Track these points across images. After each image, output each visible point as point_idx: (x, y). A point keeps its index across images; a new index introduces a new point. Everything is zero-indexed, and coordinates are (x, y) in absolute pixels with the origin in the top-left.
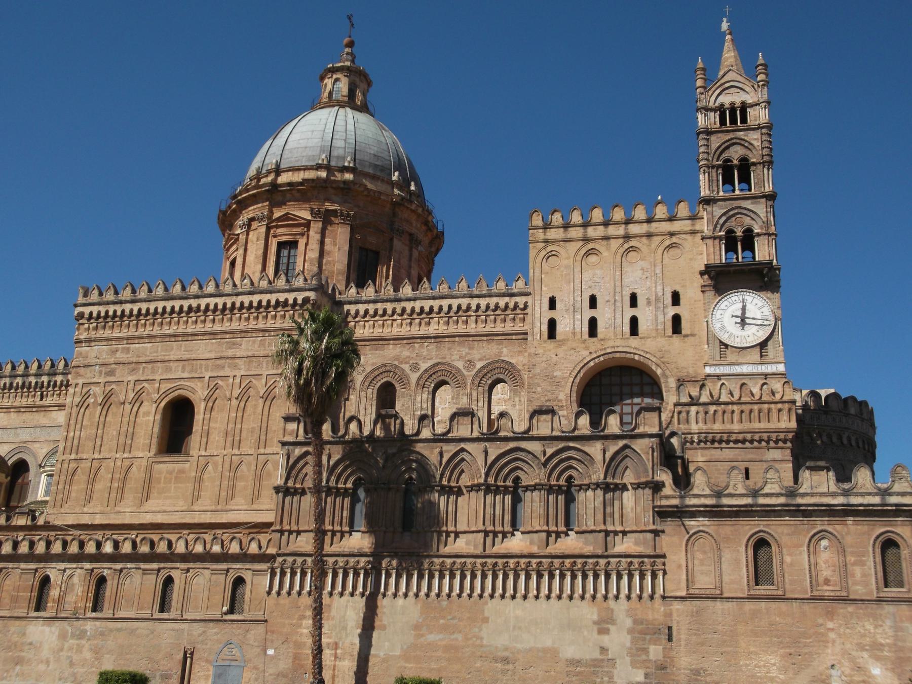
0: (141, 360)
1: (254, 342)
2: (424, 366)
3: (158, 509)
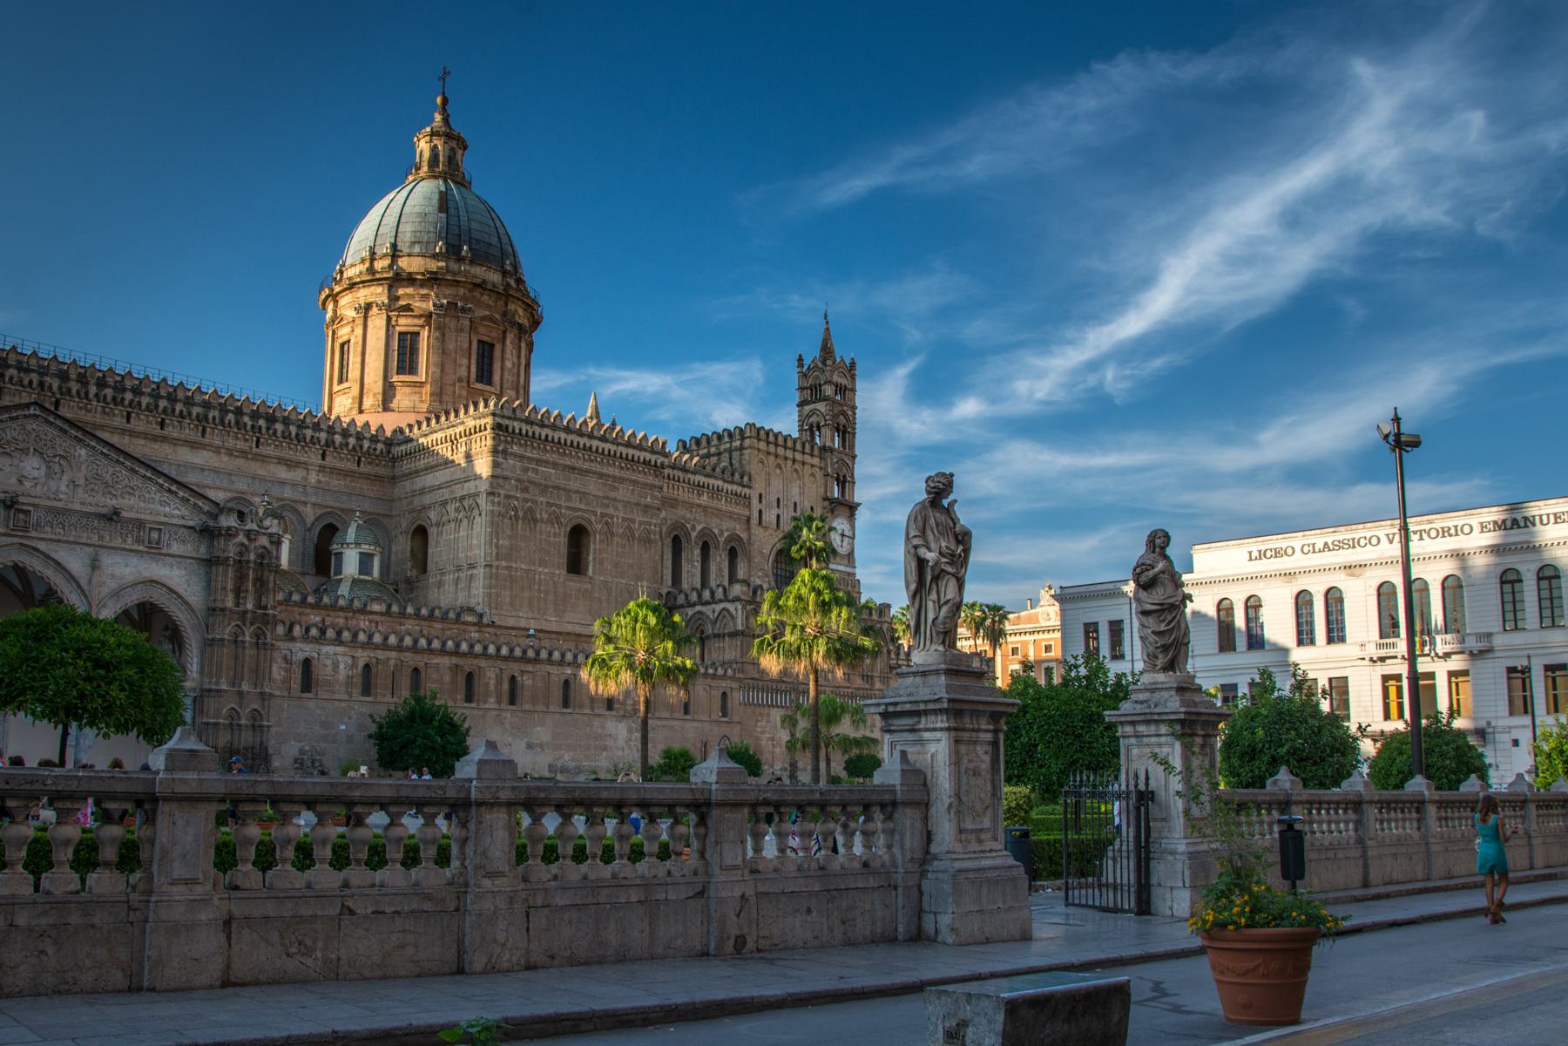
0: (549, 483)
2: (699, 528)
3: (576, 621)
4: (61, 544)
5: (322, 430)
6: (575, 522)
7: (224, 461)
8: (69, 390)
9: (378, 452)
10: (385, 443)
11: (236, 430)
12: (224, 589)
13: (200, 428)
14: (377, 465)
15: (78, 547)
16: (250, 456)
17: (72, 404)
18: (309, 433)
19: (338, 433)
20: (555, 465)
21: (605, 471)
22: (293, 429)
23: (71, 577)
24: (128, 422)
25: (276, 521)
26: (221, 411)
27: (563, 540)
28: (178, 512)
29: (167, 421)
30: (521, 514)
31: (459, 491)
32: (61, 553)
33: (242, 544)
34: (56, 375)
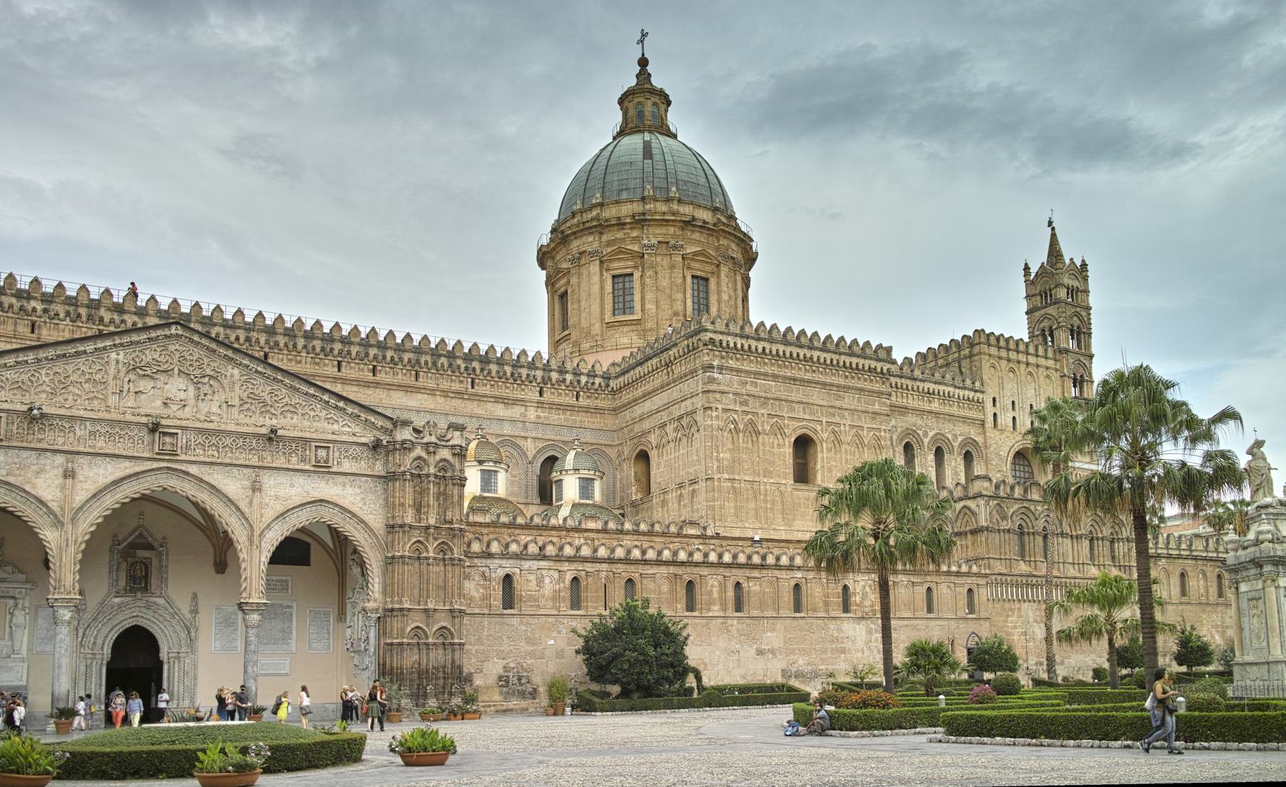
0: (769, 395)
1: (853, 398)
4: (216, 467)
5: (537, 368)
6: (799, 432)
7: (439, 403)
8: (277, 344)
9: (596, 386)
10: (603, 377)
11: (449, 373)
12: (402, 505)
13: (414, 373)
14: (597, 398)
15: (235, 470)
16: (466, 397)
17: (281, 356)
18: (524, 372)
19: (554, 370)
20: (775, 377)
21: (828, 380)
22: (508, 370)
23: (229, 501)
24: (339, 370)
25: (457, 433)
26: (432, 355)
27: (788, 450)
28: (349, 430)
29: (379, 368)
30: (741, 427)
31: (676, 411)
32: (215, 476)
33: (419, 458)
34: (262, 331)
